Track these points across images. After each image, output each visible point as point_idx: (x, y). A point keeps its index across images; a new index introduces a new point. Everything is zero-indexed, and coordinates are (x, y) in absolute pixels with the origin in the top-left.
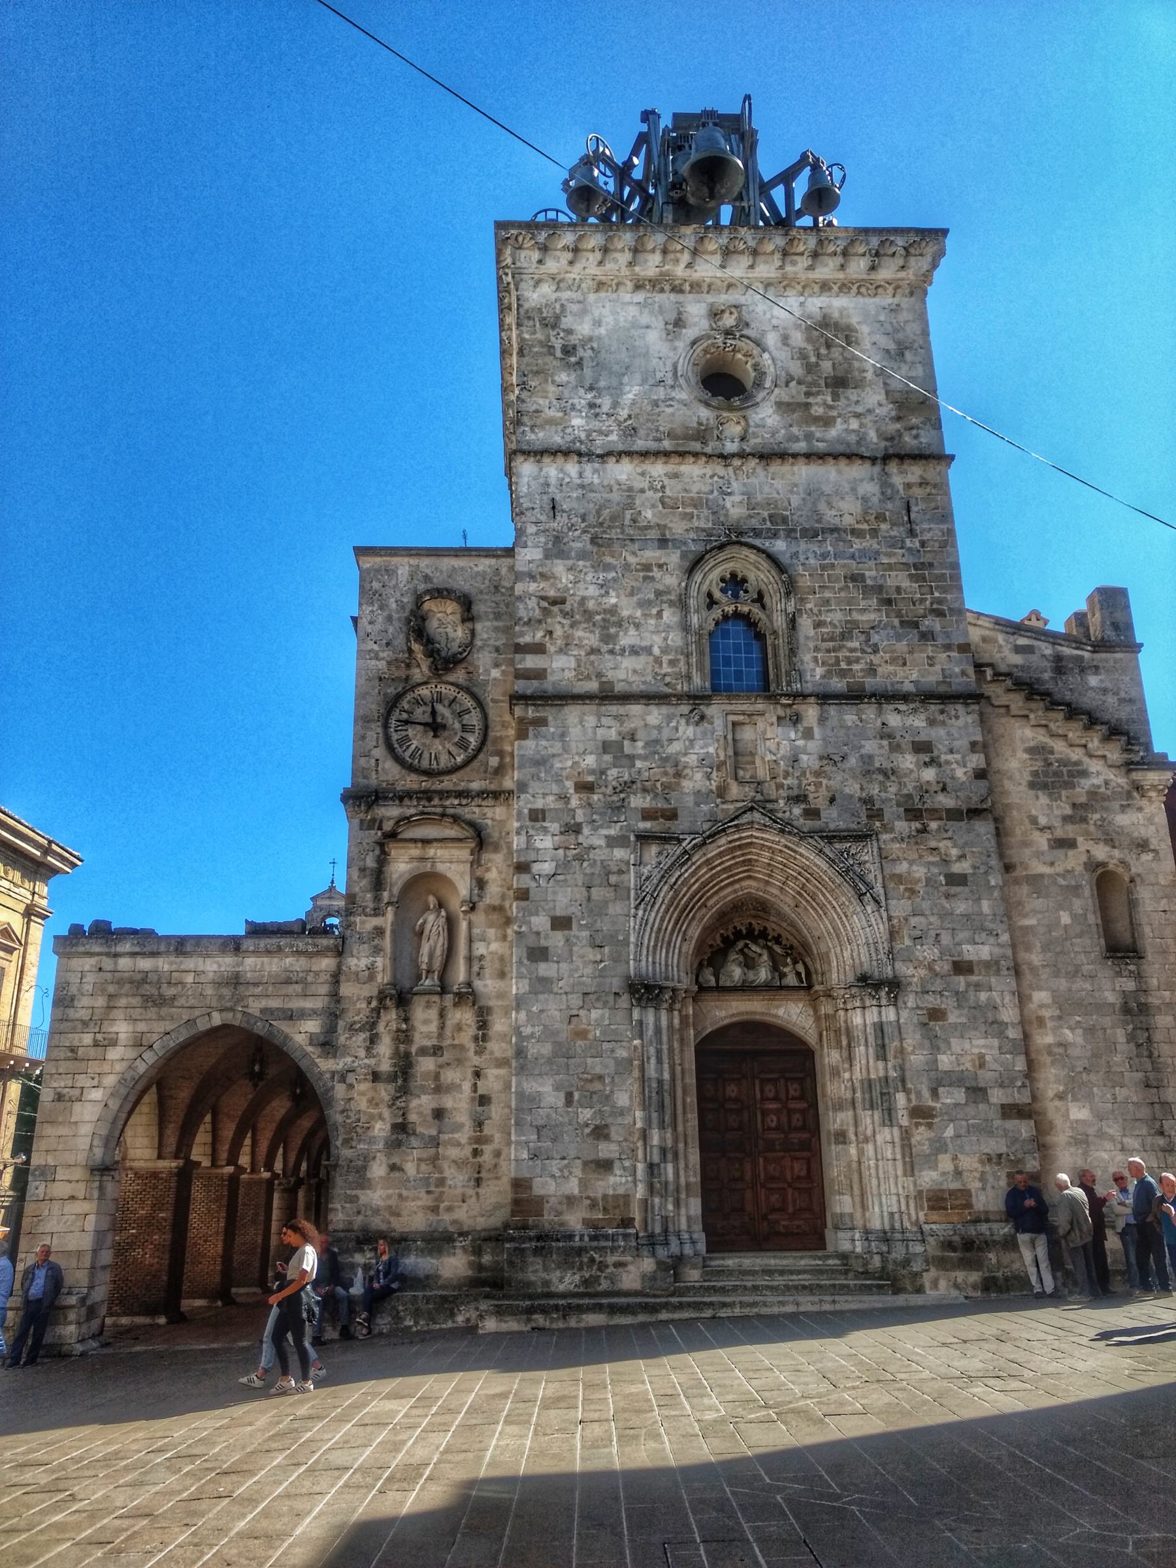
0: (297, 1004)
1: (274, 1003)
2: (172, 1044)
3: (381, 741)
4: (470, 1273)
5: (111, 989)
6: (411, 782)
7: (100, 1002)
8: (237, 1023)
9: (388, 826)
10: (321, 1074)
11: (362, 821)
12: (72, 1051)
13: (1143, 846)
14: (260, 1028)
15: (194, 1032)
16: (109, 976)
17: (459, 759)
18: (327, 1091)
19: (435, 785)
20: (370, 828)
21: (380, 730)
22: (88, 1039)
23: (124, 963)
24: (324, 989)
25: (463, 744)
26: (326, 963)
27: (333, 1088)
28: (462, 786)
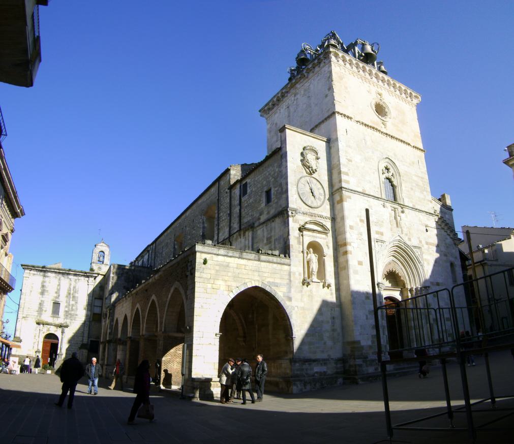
0: (278, 281)
1: (271, 280)
2: (239, 292)
3: (297, 193)
4: (335, 371)
5: (217, 268)
6: (304, 208)
7: (213, 272)
8: (260, 286)
9: (302, 223)
10: (288, 306)
11: (293, 219)
12: (205, 290)
13: (456, 258)
14: (268, 289)
15: (246, 288)
16: (216, 263)
17: (319, 204)
18: (290, 313)
19: (312, 211)
20: (295, 222)
21: (296, 189)
22: (210, 286)
23: (220, 258)
24: (287, 277)
25: (319, 199)
26: (286, 267)
27: (292, 311)
28: (320, 213)
